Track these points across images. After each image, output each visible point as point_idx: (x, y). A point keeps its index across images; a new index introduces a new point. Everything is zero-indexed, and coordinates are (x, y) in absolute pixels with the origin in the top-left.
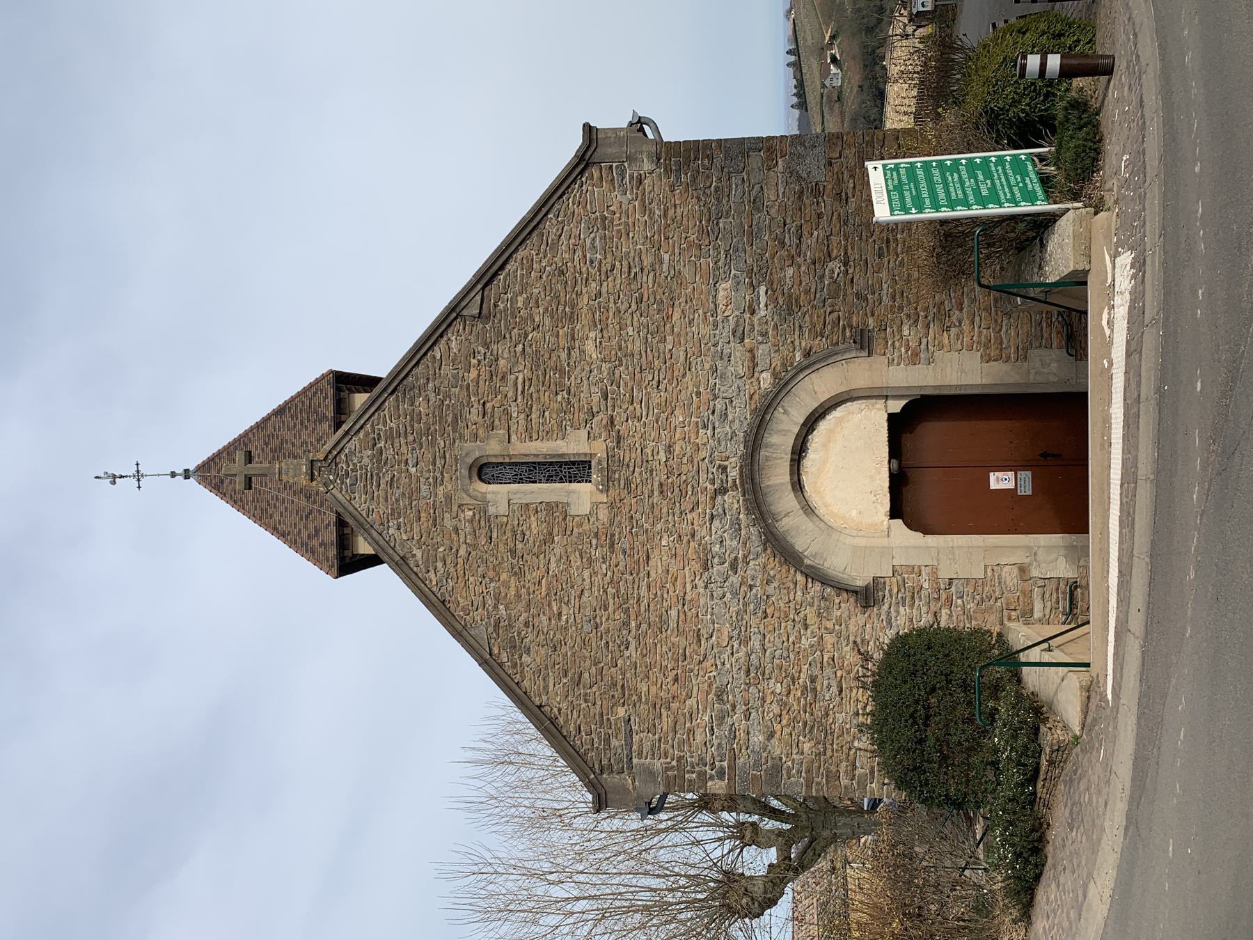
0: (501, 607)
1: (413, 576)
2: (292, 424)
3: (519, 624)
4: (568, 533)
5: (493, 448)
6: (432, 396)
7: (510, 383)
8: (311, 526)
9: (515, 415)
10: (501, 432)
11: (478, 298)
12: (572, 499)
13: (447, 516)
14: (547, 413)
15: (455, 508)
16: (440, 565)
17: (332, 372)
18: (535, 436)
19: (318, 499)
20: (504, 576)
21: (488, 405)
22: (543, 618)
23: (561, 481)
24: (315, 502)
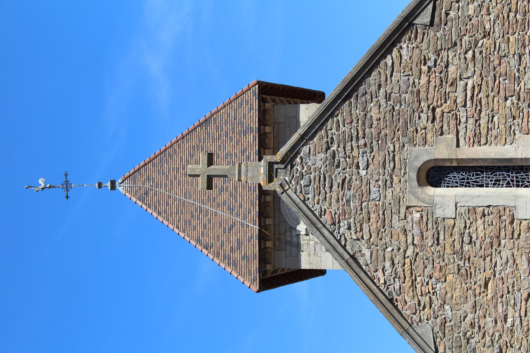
0: (447, 307)
1: (362, 275)
2: (216, 135)
3: (466, 324)
4: (516, 236)
5: (443, 150)
6: (383, 102)
7: (460, 89)
8: (233, 239)
9: (463, 120)
10: (450, 136)
11: (430, 7)
12: (520, 204)
13: (395, 217)
14: (495, 119)
15: (403, 210)
16: (388, 264)
17: (259, 83)
18: (483, 141)
19: (242, 211)
20: (450, 278)
21: (438, 111)
22: (488, 319)
23: (508, 185)
24: (238, 215)
